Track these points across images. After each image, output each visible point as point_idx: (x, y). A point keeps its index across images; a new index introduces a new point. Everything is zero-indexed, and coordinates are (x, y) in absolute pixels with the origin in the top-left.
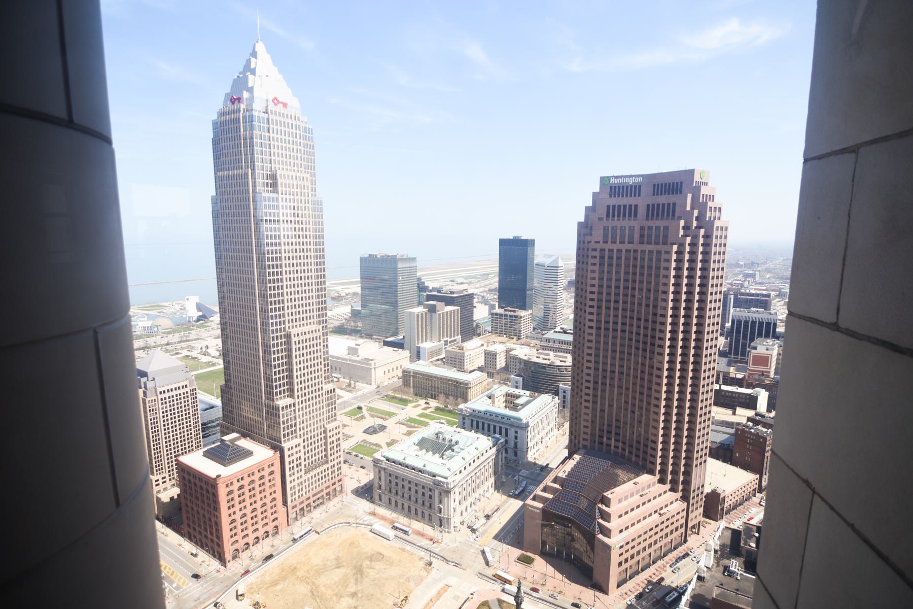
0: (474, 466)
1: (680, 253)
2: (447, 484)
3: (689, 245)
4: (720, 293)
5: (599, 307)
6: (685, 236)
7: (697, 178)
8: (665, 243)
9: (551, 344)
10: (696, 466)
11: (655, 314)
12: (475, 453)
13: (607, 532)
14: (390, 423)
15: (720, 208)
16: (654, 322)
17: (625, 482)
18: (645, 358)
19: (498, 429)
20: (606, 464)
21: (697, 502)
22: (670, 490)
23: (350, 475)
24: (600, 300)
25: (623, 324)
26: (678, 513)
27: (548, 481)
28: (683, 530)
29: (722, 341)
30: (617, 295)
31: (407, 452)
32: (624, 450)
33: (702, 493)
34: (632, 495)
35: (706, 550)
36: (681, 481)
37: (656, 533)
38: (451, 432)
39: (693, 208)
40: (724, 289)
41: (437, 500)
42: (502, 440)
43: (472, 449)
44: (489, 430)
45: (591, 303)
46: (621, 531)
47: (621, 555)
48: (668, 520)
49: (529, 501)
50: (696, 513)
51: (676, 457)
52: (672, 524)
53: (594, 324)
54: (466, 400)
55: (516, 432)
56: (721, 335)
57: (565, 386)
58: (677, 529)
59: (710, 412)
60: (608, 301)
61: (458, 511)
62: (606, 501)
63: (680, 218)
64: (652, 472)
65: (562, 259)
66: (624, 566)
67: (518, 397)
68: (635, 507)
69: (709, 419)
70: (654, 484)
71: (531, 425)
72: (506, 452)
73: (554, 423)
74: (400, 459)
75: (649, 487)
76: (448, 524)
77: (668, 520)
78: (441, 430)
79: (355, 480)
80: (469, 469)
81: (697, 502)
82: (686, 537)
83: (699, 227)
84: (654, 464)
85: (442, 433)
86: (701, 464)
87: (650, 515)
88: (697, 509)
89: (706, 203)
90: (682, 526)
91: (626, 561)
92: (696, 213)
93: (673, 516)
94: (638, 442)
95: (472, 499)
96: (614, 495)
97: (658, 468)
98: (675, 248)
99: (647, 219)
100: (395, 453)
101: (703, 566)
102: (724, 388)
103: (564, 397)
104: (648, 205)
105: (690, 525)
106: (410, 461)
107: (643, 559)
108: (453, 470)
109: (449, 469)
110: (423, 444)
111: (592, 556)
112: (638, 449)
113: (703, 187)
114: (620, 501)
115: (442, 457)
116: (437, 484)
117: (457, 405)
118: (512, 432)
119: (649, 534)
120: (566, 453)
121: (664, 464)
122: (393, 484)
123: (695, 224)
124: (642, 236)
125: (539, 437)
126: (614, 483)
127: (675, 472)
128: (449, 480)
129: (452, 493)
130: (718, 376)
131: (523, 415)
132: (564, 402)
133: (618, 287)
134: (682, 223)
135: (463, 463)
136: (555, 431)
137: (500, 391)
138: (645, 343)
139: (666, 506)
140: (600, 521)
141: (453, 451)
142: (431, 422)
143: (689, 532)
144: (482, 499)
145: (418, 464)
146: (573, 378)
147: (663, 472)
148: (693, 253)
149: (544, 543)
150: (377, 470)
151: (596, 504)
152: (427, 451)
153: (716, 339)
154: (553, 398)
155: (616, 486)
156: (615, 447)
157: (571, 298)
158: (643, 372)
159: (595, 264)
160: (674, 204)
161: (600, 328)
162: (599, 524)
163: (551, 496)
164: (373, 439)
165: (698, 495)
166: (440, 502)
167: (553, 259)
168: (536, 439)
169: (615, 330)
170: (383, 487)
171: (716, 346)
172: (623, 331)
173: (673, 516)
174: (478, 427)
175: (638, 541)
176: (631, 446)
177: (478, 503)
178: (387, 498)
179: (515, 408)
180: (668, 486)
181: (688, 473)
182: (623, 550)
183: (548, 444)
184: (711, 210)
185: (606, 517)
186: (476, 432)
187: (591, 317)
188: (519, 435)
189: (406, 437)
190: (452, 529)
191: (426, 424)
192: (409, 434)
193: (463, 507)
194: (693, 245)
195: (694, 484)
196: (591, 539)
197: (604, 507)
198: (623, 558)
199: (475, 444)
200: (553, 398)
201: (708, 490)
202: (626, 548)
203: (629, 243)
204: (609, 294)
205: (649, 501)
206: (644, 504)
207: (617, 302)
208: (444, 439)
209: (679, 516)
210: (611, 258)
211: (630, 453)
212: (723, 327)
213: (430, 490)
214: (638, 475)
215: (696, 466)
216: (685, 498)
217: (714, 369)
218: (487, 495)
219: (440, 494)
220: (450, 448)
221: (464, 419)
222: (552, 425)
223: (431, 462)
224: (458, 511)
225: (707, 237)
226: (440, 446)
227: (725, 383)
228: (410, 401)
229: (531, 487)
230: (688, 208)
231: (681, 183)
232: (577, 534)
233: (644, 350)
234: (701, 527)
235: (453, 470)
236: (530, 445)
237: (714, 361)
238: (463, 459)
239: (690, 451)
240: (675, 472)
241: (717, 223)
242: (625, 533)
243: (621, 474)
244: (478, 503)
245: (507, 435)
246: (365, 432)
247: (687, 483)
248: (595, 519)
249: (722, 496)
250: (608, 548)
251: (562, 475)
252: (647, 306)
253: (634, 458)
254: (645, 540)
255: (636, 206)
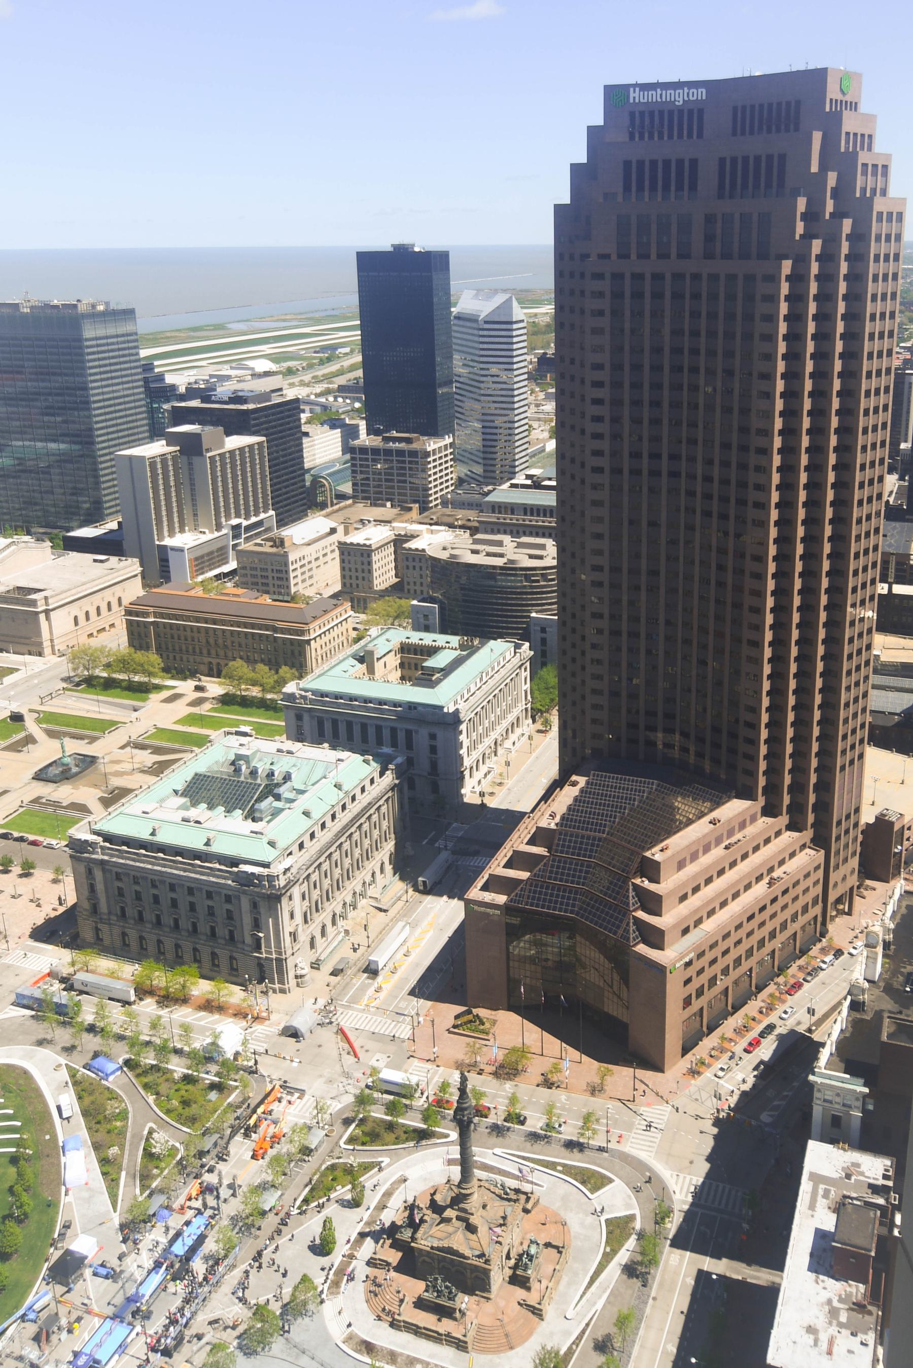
0: (334, 827)
1: (798, 278)
2: (271, 878)
3: (819, 258)
4: (888, 371)
5: (616, 420)
6: (808, 236)
7: (833, 92)
8: (763, 256)
9: (509, 519)
10: (843, 768)
11: (744, 430)
12: (334, 797)
13: (655, 938)
14: (105, 748)
15: (885, 167)
16: (744, 449)
17: (690, 822)
18: (726, 534)
19: (386, 733)
20: (643, 788)
21: (846, 846)
22: (790, 827)
23: (10, 891)
24: (617, 403)
25: (674, 457)
26: (807, 876)
27: (519, 841)
28: (817, 910)
29: (892, 482)
30: (657, 386)
31: (157, 813)
32: (685, 750)
33: (856, 825)
34: (707, 849)
35: (867, 946)
36: (811, 805)
37: (762, 924)
38: (268, 750)
39: (824, 167)
40: (896, 363)
41: (247, 920)
42: (399, 760)
43: (326, 786)
44: (365, 740)
45: (596, 410)
46: (686, 931)
47: (688, 981)
48: (785, 892)
49: (475, 893)
50: (844, 870)
51: (800, 755)
52: (796, 899)
53: (604, 462)
54: (300, 668)
55: (433, 737)
56: (890, 472)
57: (543, 615)
58: (805, 909)
59: (869, 647)
60: (636, 403)
61: (303, 938)
62: (652, 871)
63: (796, 193)
64: (747, 794)
65: (522, 302)
66: (696, 1005)
67: (432, 651)
68: (715, 870)
69: (867, 663)
70: (753, 819)
71: (464, 715)
72: (412, 786)
73: (522, 706)
74: (144, 834)
75: (743, 826)
76: (281, 971)
77: (785, 892)
78: (243, 751)
79: (23, 902)
80: (323, 837)
81: (846, 846)
82: (824, 924)
83: (838, 215)
84: (752, 774)
85: (246, 758)
86: (852, 762)
87: (748, 887)
88: (846, 860)
89: (855, 154)
90: (815, 902)
91: (700, 992)
92: (832, 179)
93: (797, 883)
94: (716, 730)
95: (335, 906)
96: (669, 853)
97: (762, 781)
98: (787, 267)
99: (721, 196)
100: (125, 822)
101: (861, 980)
102: (899, 589)
103: (544, 641)
104: (722, 161)
105: (832, 896)
106: (168, 836)
107: (736, 983)
108: (281, 844)
109: (272, 844)
110: (199, 790)
111: (625, 995)
112: (716, 745)
113: (846, 114)
114: (681, 865)
115: (252, 816)
116: (247, 880)
117: (283, 682)
118: (422, 737)
119: (747, 927)
120: (552, 771)
121: (774, 772)
122: (129, 899)
123: (830, 206)
124: (709, 238)
125: (488, 741)
126: (670, 827)
127: (798, 788)
128: (277, 869)
129: (284, 900)
130: (885, 563)
131: (443, 696)
132: (544, 654)
133: (657, 368)
134: (801, 204)
135: (305, 824)
136: (528, 726)
137: (387, 640)
138: (724, 499)
139: (782, 863)
140: (641, 914)
141: (278, 797)
142: (213, 734)
143: (832, 912)
144: (363, 903)
145: (192, 840)
146: (562, 594)
147: (773, 790)
148: (827, 278)
149: (512, 984)
150: (82, 868)
151: (626, 880)
152: (211, 807)
153: (881, 479)
154: (517, 647)
155: (670, 833)
156: (666, 745)
157: (548, 397)
158: (721, 568)
159: (601, 313)
160: (782, 158)
161: (620, 471)
162: (637, 921)
163: (524, 875)
164: (64, 793)
165: (847, 832)
166: (257, 925)
167: (500, 299)
168: (481, 748)
169: (655, 473)
170: (103, 907)
171: (880, 496)
172: (674, 474)
173: (797, 883)
174: (336, 735)
175: (722, 947)
176: (701, 740)
177: (351, 914)
178: (117, 931)
179: (428, 678)
180: (784, 820)
181: (825, 787)
182: (692, 971)
183: (512, 757)
184: (865, 173)
185: (653, 903)
186: (333, 747)
187: (597, 445)
188: (439, 743)
189: (152, 779)
190: (292, 982)
191: (202, 742)
192: (158, 769)
193: (314, 928)
194: (828, 258)
195: (838, 811)
196: (622, 962)
197: (646, 884)
198: (692, 988)
199: (333, 778)
200: (517, 647)
201: (868, 817)
202: (697, 965)
203: (680, 256)
204: (636, 386)
205: (745, 856)
206: (733, 864)
207: (656, 404)
208: (254, 773)
209: (810, 882)
210: (638, 295)
211: (700, 755)
212: (895, 450)
213: (228, 899)
214: (717, 804)
215: (843, 768)
216: (821, 840)
217: (876, 548)
218: (372, 891)
219: (255, 905)
220: (271, 790)
221: (299, 717)
222: (517, 711)
223: (228, 833)
224: (303, 938)
225: (859, 237)
226: (243, 791)
227: (900, 580)
228: (158, 688)
229: (474, 862)
230: (814, 168)
231: (798, 103)
232: (588, 952)
233: (724, 517)
234: (857, 899)
235: (281, 844)
236: (467, 762)
237: (877, 530)
238: (306, 814)
239: (828, 738)
240: (798, 788)
241: (879, 205)
242: (695, 936)
243: (683, 806)
244: (351, 914)
245: (409, 746)
246: (41, 776)
247: (824, 807)
248: (626, 912)
249: (896, 828)
250: (660, 970)
251: (546, 822)
252: (727, 410)
253: (707, 767)
254: (739, 942)
255: (694, 163)
